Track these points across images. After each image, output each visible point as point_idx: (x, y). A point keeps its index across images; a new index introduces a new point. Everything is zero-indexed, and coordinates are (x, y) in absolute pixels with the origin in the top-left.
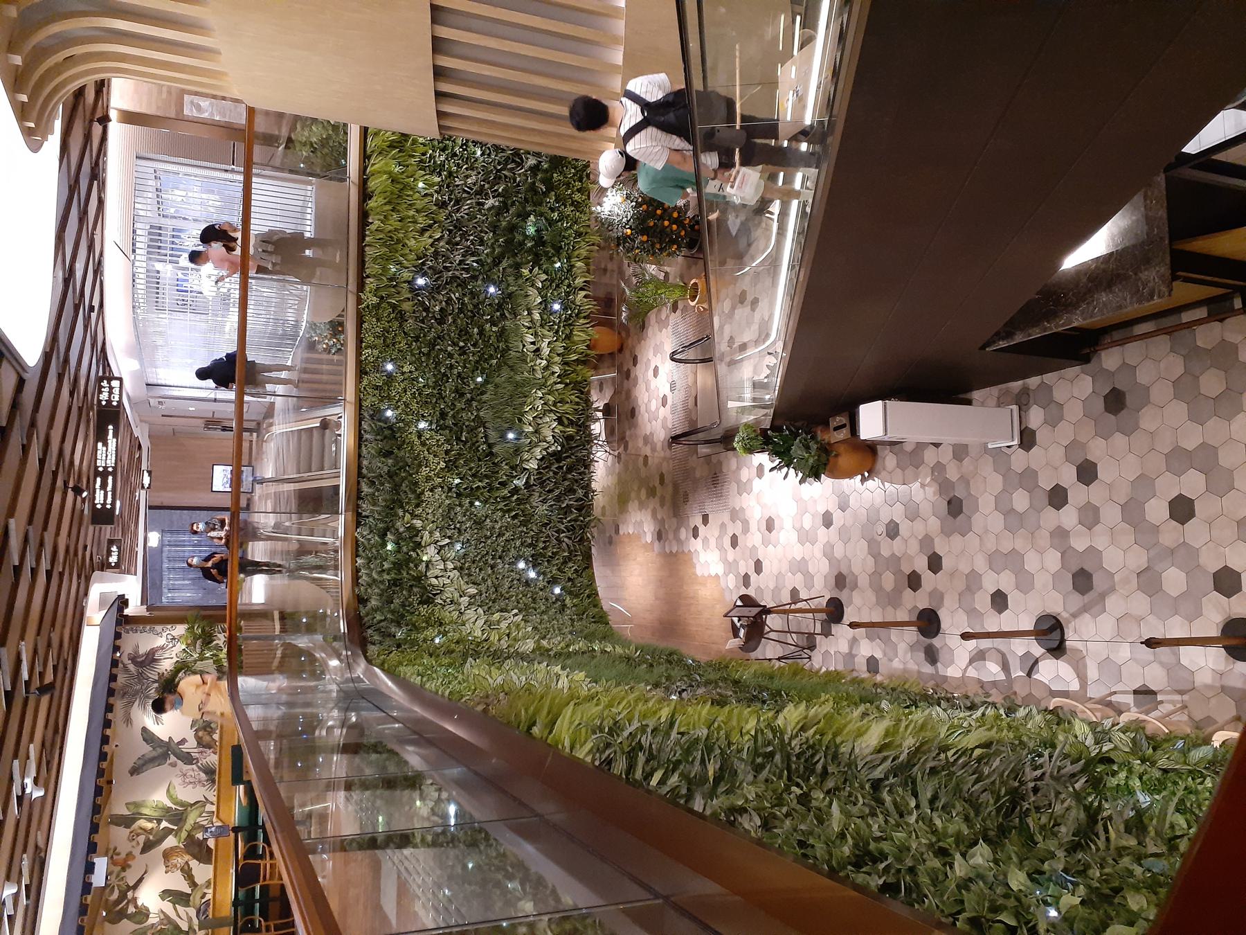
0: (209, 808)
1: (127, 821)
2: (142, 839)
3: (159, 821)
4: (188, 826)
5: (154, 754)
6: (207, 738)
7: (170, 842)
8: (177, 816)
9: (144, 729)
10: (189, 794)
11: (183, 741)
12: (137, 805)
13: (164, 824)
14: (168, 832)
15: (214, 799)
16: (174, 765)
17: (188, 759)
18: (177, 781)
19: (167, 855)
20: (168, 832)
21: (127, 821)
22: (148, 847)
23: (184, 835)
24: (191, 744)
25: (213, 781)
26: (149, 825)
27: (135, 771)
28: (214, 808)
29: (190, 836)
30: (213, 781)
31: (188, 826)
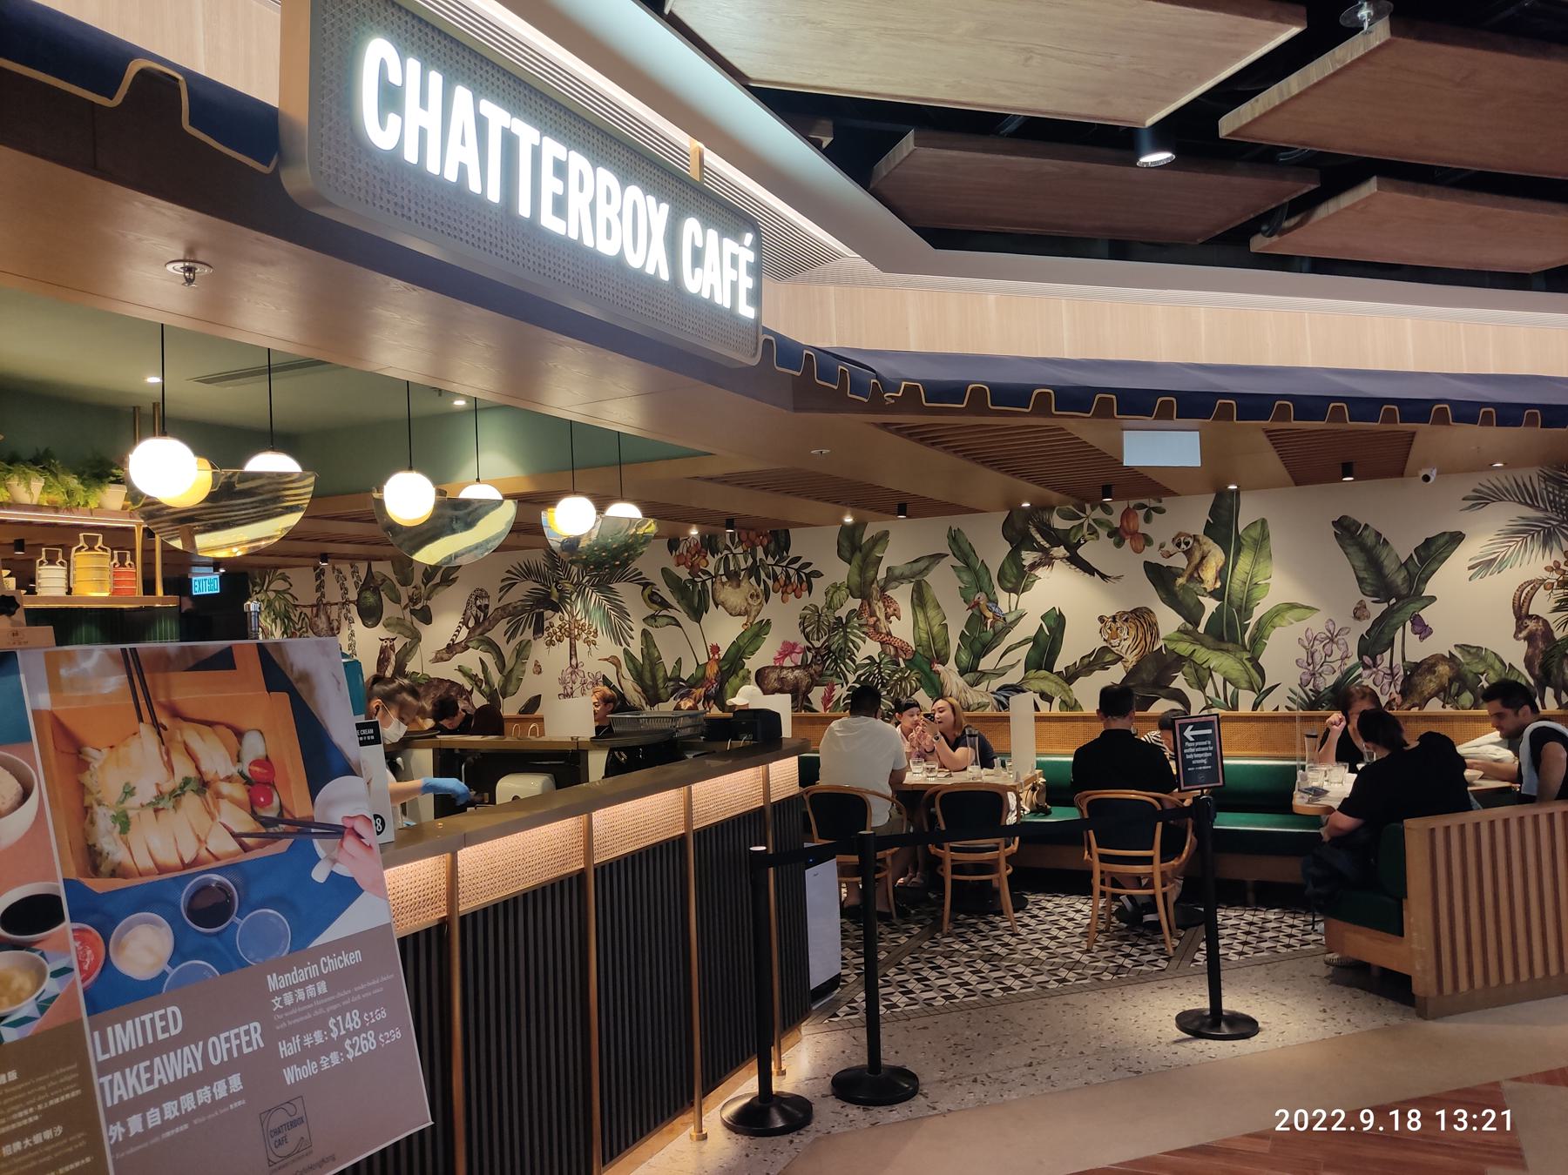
0: (1246, 700)
1: (1221, 527)
2: (1180, 561)
3: (1217, 594)
4: (1202, 655)
5: (1390, 566)
6: (1430, 684)
7: (1169, 621)
8: (1232, 630)
9: (1456, 538)
10: (1282, 657)
11: (1423, 630)
12: (1261, 542)
13: (1210, 605)
14: (1191, 614)
15: (1267, 708)
16: (1359, 613)
17: (1374, 644)
18: (1317, 624)
19: (1140, 617)
20: (1191, 614)
21: (1221, 527)
22: (1160, 577)
23: (1184, 648)
24: (1416, 649)
25: (1312, 705)
26: (1209, 574)
27: (1347, 531)
28: (1245, 708)
29: (1178, 661)
30: (1312, 705)
31: (1202, 655)
